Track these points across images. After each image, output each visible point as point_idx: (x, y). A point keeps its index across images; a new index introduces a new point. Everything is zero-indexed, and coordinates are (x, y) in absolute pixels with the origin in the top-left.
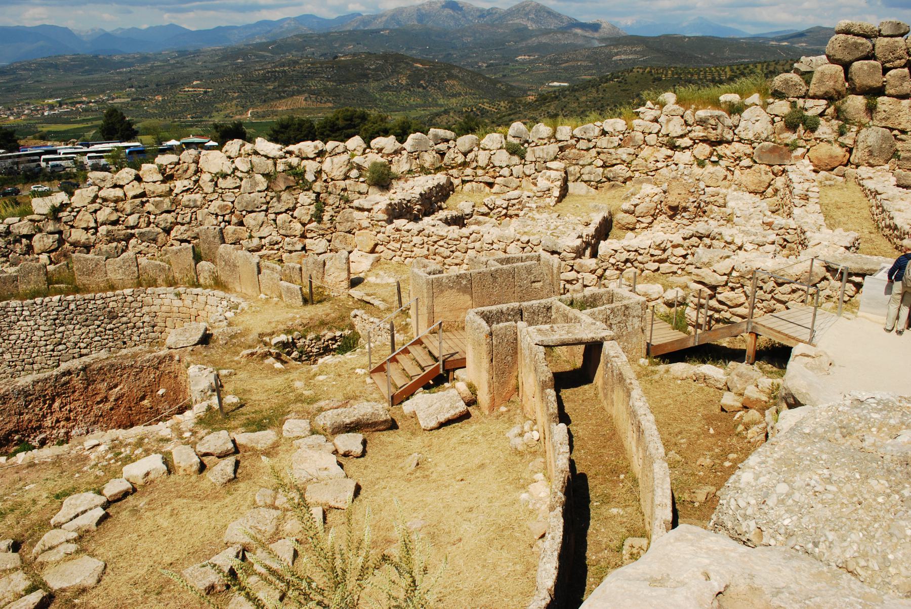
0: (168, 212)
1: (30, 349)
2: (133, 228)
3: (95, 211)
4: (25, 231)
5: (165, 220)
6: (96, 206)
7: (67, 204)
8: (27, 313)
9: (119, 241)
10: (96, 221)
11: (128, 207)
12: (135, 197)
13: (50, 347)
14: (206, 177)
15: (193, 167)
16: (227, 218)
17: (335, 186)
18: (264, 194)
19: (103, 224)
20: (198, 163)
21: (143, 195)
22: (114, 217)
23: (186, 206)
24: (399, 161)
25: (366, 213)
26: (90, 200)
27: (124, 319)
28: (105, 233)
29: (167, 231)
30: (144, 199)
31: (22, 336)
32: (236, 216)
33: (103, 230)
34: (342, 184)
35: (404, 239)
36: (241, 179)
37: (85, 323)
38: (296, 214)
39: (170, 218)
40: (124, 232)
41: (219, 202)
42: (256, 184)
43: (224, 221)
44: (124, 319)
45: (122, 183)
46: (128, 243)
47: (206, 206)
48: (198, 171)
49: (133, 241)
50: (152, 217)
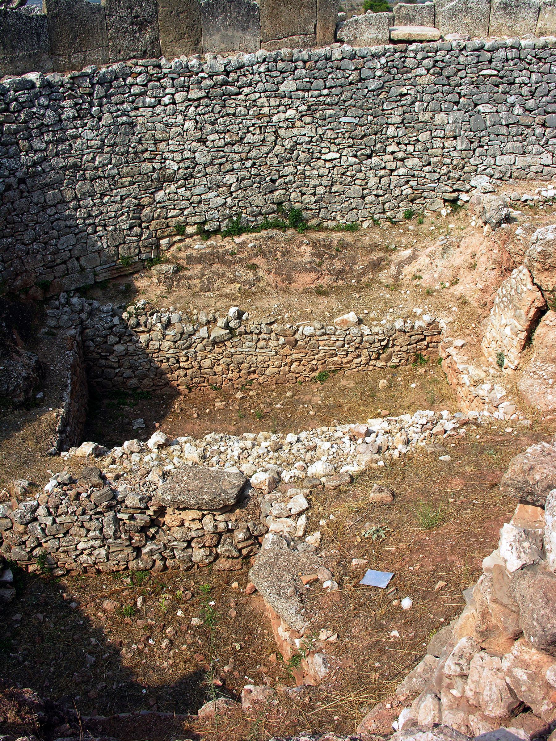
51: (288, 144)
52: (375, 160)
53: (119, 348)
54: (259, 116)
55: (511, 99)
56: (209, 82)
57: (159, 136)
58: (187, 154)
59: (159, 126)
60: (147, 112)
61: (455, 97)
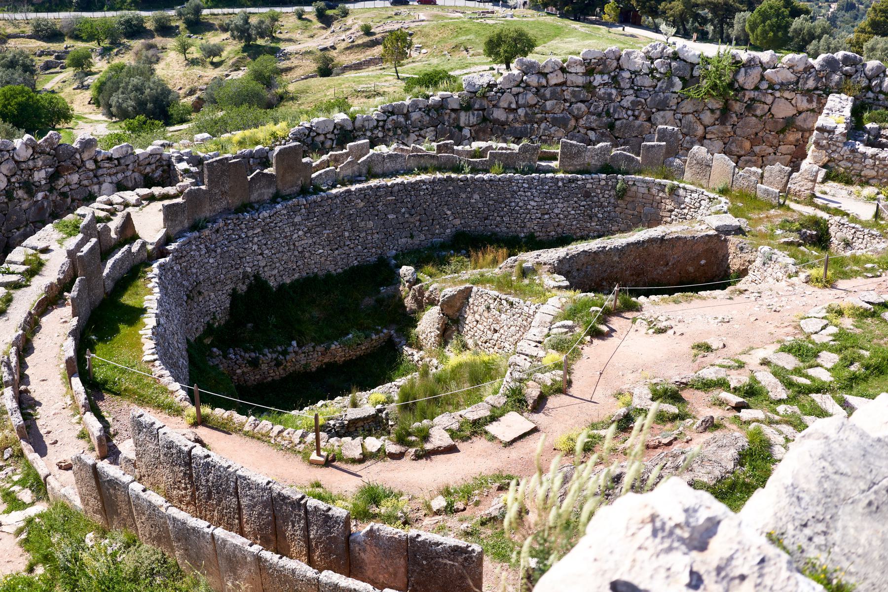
0: (582, 101)
1: (524, 215)
2: (547, 112)
3: (518, 94)
4: (456, 106)
5: (579, 109)
6: (521, 90)
7: (495, 85)
8: (526, 185)
9: (532, 122)
10: (517, 102)
11: (548, 93)
12: (555, 85)
13: (539, 215)
14: (626, 75)
15: (615, 64)
16: (636, 113)
17: (744, 96)
18: (676, 96)
19: (524, 106)
20: (618, 59)
21: (564, 83)
22: (534, 102)
23: (600, 98)
24: (808, 78)
25: (826, 135)
26: (516, 83)
27: (595, 199)
28: (522, 114)
29: (577, 118)
30: (564, 88)
31: (521, 204)
32: (646, 112)
33: (521, 112)
34: (752, 94)
35: (856, 160)
36: (659, 80)
37: (566, 199)
38: (702, 116)
39: (582, 106)
40: (539, 116)
41: (633, 98)
42: (671, 84)
43: (633, 115)
44: (595, 199)
45: (546, 71)
46: (539, 126)
47: (619, 99)
48: (620, 68)
49: (543, 125)
50: (568, 104)
51: (300, 249)
52: (341, 251)
53: (239, 371)
54: (286, 237)
55: (403, 210)
56: (263, 224)
57: (241, 255)
58: (256, 263)
59: (241, 250)
60: (234, 243)
61: (375, 212)
